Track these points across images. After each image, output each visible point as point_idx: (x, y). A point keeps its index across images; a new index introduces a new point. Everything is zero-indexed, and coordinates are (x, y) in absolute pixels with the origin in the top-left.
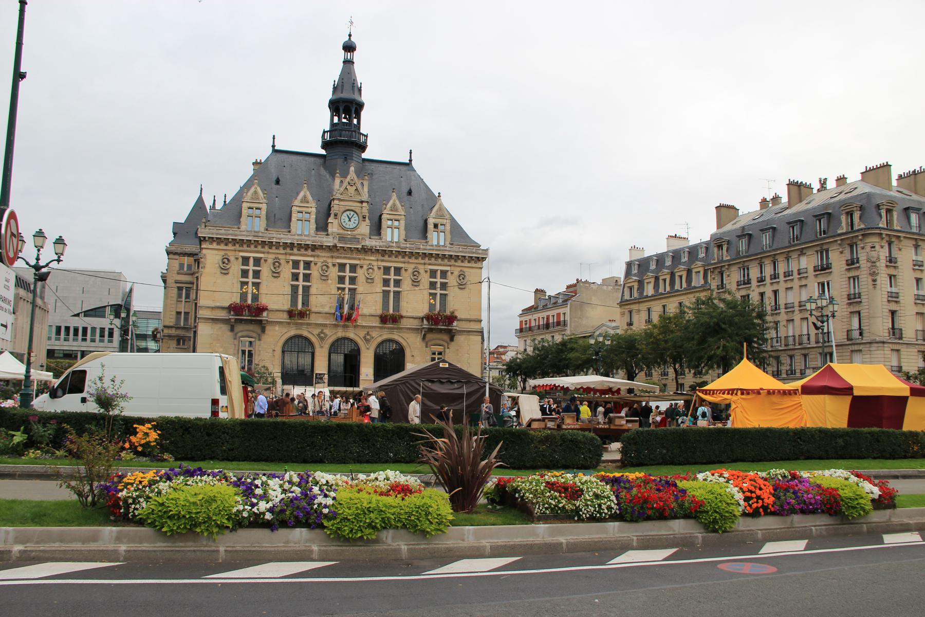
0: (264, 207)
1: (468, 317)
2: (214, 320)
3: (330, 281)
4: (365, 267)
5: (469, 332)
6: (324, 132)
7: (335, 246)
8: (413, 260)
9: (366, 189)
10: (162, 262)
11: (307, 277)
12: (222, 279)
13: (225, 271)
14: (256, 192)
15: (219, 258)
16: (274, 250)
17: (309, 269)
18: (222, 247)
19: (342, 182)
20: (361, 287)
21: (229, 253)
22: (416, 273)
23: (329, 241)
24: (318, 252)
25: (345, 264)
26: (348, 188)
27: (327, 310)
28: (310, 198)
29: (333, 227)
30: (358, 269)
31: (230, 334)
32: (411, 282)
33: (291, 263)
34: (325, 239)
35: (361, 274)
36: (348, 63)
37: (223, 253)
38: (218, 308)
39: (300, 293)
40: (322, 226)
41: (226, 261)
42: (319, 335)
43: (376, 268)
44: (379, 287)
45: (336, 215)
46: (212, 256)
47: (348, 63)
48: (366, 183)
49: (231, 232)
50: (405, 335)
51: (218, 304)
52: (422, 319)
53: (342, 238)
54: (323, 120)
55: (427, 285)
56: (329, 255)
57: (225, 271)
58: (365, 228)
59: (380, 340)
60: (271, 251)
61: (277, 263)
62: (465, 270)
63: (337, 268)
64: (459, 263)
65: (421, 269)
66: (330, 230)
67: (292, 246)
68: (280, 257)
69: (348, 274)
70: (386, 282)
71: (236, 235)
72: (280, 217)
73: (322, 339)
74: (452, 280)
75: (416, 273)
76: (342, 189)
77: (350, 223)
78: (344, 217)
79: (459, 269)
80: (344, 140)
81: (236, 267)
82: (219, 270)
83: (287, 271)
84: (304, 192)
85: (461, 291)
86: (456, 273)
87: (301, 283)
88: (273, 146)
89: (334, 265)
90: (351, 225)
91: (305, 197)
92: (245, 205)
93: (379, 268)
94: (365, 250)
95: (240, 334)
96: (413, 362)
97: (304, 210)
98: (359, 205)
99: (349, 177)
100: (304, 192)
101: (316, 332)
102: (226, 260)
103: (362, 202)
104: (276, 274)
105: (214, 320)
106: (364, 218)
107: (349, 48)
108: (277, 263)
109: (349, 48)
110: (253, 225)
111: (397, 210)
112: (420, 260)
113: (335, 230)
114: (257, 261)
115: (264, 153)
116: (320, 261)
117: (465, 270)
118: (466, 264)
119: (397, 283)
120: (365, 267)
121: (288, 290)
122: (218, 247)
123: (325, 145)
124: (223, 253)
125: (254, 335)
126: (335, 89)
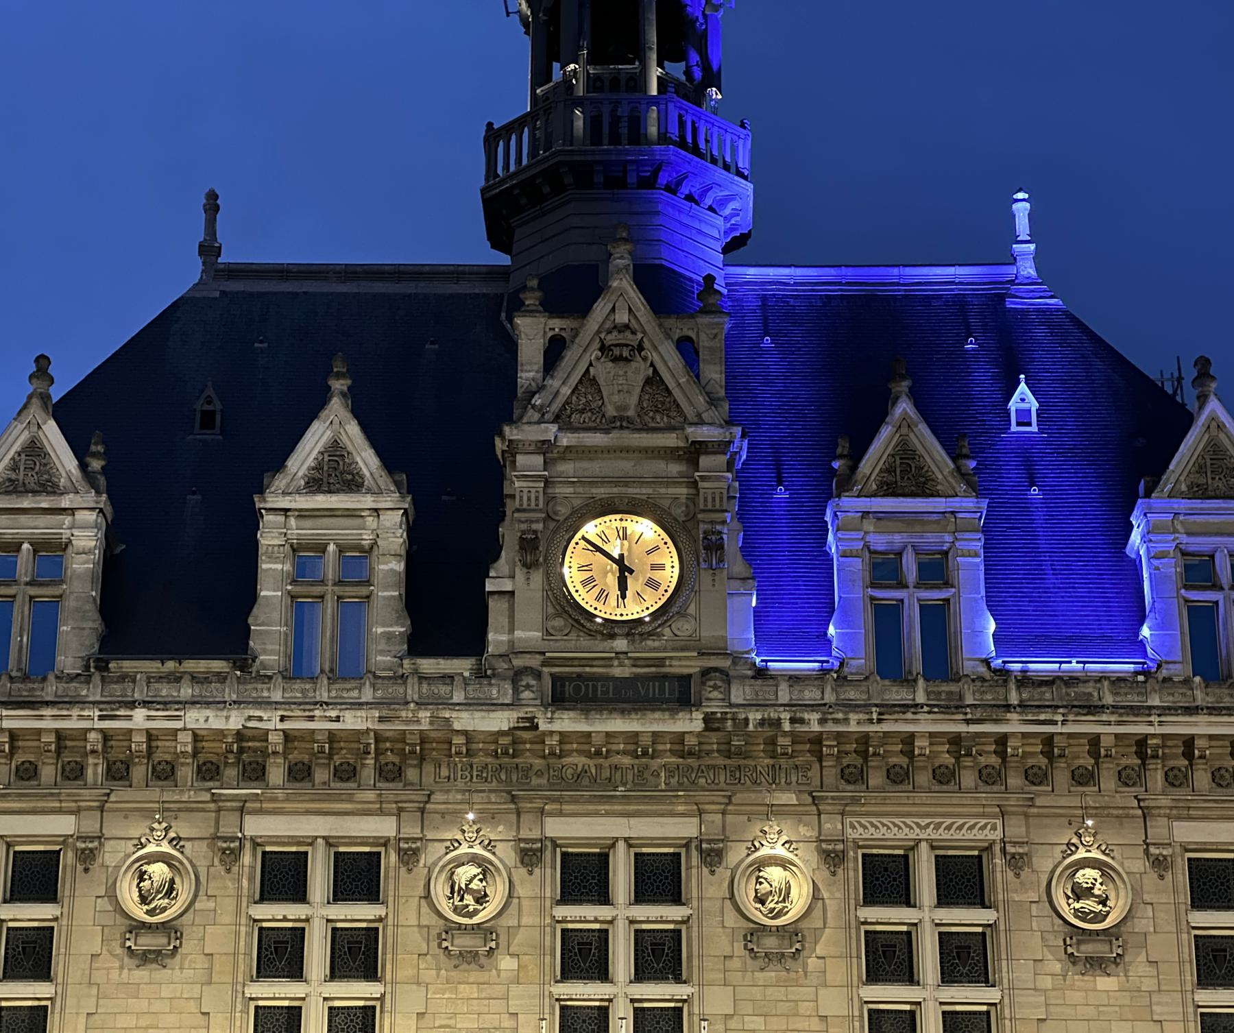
6: (493, 136)
19: (555, 351)
28: (367, 460)
30: (694, 875)
63: (550, 877)
66: (496, 638)
76: (562, 386)
84: (334, 428)
88: (209, 250)
91: (335, 451)
99: (600, 309)
100: (334, 428)
106: (715, 547)
113: (528, 635)
123: (504, 211)
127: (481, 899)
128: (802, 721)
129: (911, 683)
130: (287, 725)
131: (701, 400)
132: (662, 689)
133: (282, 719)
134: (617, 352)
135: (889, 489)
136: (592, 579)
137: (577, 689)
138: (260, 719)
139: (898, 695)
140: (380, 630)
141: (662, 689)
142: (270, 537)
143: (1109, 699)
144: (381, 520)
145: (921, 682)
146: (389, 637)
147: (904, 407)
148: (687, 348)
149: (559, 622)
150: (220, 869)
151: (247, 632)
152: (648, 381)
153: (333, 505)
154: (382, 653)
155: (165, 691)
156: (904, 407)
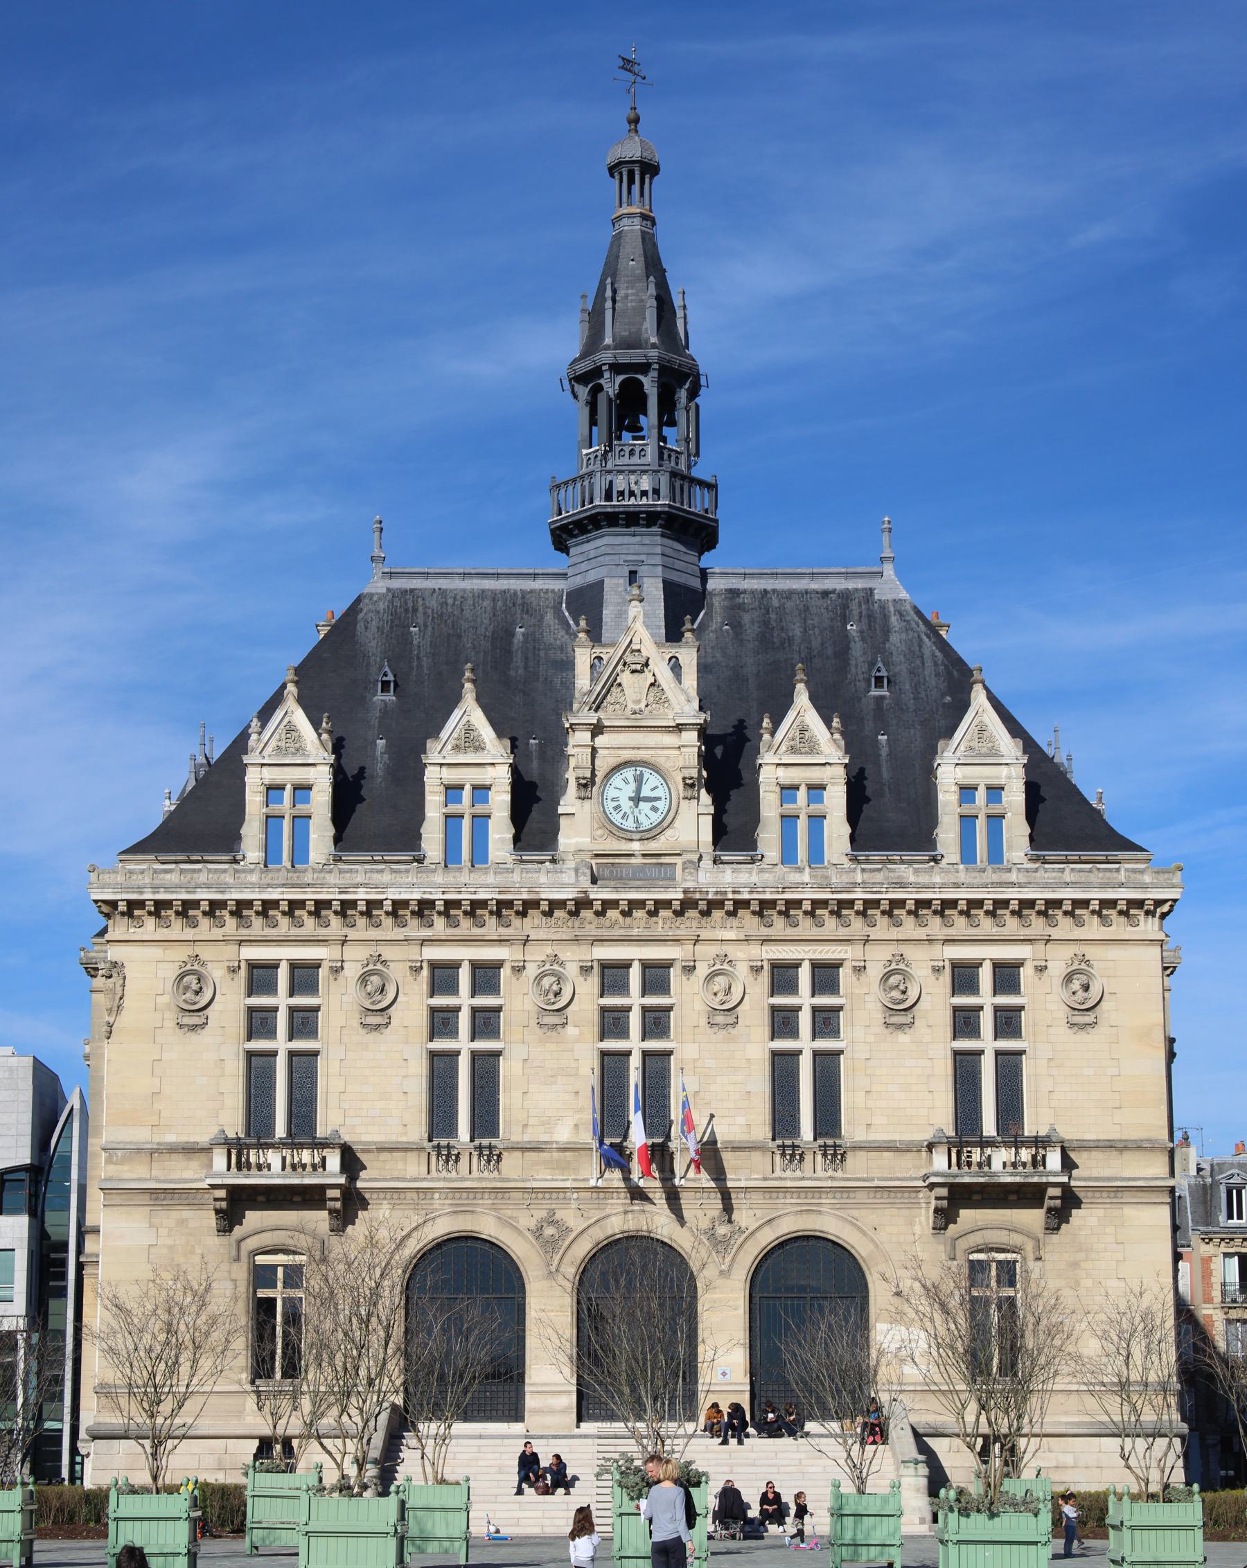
0: (322, 779)
1: (1113, 1134)
2: (161, 1196)
3: (571, 1030)
4: (702, 970)
5: (1119, 1192)
7: (583, 903)
8: (882, 928)
9: (690, 679)
11: (486, 1022)
12: (180, 1049)
13: (194, 1014)
14: (291, 729)
15: (172, 972)
16: (361, 929)
17: (494, 989)
18: (177, 930)
20: (688, 1045)
21: (205, 953)
22: (895, 974)
23: (557, 881)
24: (519, 927)
25: (626, 965)
27: (563, 1134)
28: (486, 731)
29: (578, 828)
31: (215, 1243)
32: (878, 1016)
33: (425, 972)
34: (543, 879)
35: (687, 998)
37: (182, 953)
38: (173, 1149)
41: (191, 980)
42: (538, 1232)
43: (742, 970)
44: (755, 1044)
45: (586, 785)
48: (688, 656)
49: (202, 878)
50: (868, 1217)
51: (171, 1138)
52: (930, 1147)
55: (944, 1020)
56: (565, 933)
57: (194, 1014)
58: (694, 822)
59: (767, 1237)
60: (352, 934)
62: (1091, 952)
64: (1064, 929)
65: (921, 962)
67: (424, 908)
68: (388, 952)
69: (635, 999)
70: (783, 1022)
71: (222, 888)
73: (550, 1245)
74: (1041, 999)
75: (895, 974)
78: (620, 788)
79: (1068, 951)
81: (231, 1003)
82: (170, 1018)
84: (469, 713)
85: (1082, 1036)
86: (1057, 969)
87: (463, 1044)
89: (586, 970)
90: (647, 816)
92: (254, 779)
93: (757, 970)
95: (252, 1243)
96: (898, 1317)
98: (669, 739)
100: (469, 713)
101: (527, 1220)
102: (191, 980)
103: (679, 728)
104: (377, 1015)
105: (161, 1196)
108: (373, 976)
111: (813, 749)
112: (909, 928)
114: (304, 976)
116: (536, 954)
117: (1091, 952)
118: (1093, 928)
119: (826, 1021)
120: (702, 970)
121: (419, 1070)
122: (163, 934)
124: (182, 953)
125: (303, 1241)
127: (557, 994)
128: (739, 892)
129: (801, 870)
130: (447, 896)
131: (682, 698)
132: (660, 872)
133: (443, 893)
134: (633, 667)
135: (793, 750)
136: (619, 806)
137: (612, 872)
138: (431, 893)
139: (794, 877)
140: (497, 836)
141: (660, 872)
142: (433, 778)
143: (912, 879)
144: (494, 768)
145: (807, 869)
146: (502, 840)
147: (802, 697)
148: (676, 668)
149: (600, 832)
150: (411, 979)
151: (419, 837)
152: (652, 685)
153: (468, 756)
154: (498, 850)
155: (376, 878)
156: (802, 697)
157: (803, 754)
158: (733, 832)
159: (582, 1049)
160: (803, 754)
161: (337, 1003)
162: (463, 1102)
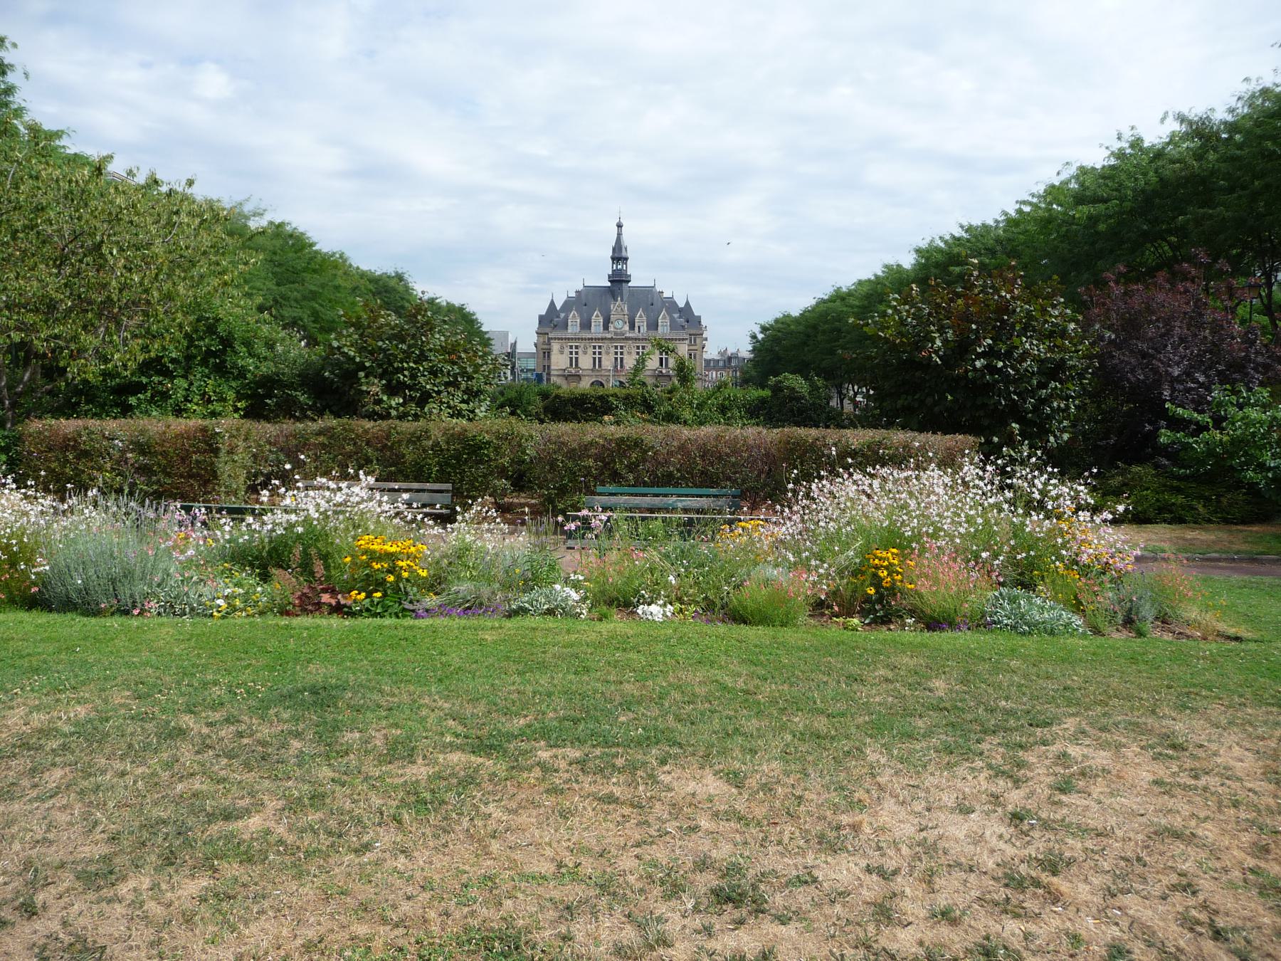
10: (535, 338)
13: (562, 353)
23: (609, 336)
26: (618, 308)
35: (625, 350)
36: (619, 235)
39: (597, 362)
40: (606, 327)
46: (555, 346)
47: (619, 235)
53: (616, 334)
54: (608, 268)
58: (627, 328)
61: (585, 348)
72: (586, 325)
77: (619, 325)
80: (619, 279)
81: (567, 350)
83: (590, 351)
94: (627, 339)
97: (597, 320)
102: (562, 348)
104: (585, 353)
107: (620, 226)
108: (585, 348)
109: (620, 226)
110: (574, 328)
114: (577, 347)
115: (580, 288)
126: (614, 249)
153: (597, 320)
157: (641, 320)
158: (632, 327)
159: (612, 357)
160: (641, 320)
161: (580, 351)
162: (597, 362)
